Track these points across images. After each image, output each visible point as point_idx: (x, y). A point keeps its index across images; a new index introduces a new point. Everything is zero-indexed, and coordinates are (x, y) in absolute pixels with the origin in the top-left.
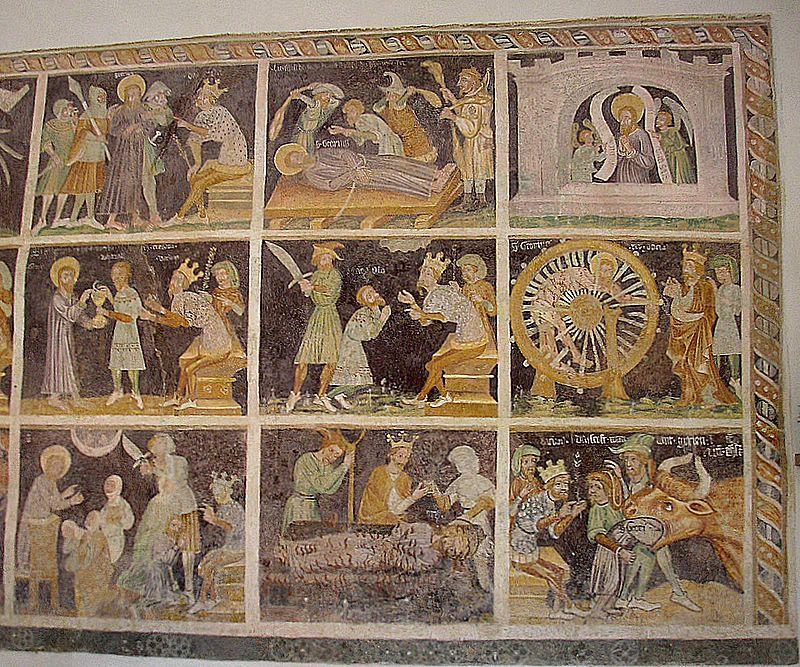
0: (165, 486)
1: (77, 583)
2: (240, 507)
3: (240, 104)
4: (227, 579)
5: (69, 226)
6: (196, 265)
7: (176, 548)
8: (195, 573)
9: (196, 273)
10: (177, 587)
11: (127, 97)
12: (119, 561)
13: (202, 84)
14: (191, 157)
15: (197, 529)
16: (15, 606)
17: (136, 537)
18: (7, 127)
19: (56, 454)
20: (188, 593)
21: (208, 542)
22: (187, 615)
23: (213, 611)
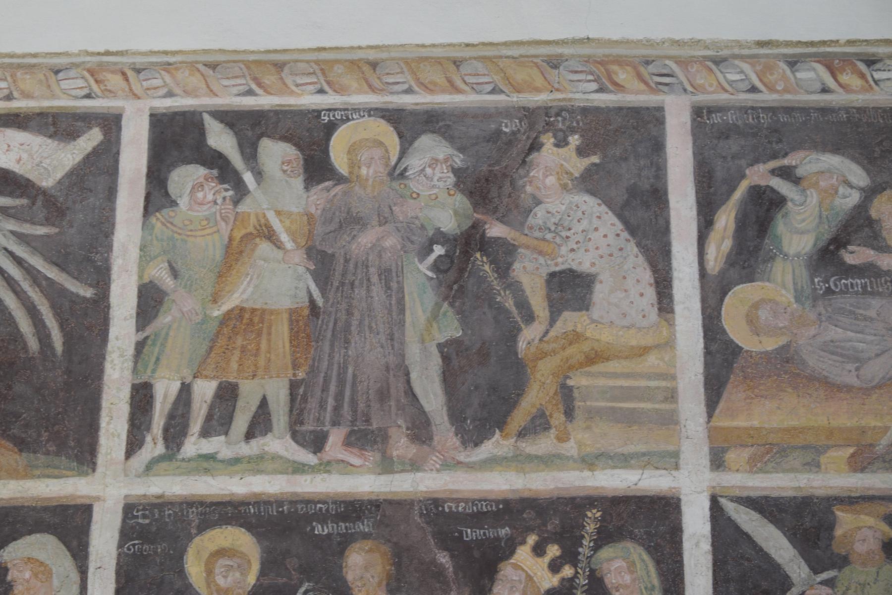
3: (633, 192)
5: (226, 453)
6: (554, 551)
9: (554, 567)
11: (353, 165)
13: (535, 146)
14: (524, 306)
18: (48, 222)
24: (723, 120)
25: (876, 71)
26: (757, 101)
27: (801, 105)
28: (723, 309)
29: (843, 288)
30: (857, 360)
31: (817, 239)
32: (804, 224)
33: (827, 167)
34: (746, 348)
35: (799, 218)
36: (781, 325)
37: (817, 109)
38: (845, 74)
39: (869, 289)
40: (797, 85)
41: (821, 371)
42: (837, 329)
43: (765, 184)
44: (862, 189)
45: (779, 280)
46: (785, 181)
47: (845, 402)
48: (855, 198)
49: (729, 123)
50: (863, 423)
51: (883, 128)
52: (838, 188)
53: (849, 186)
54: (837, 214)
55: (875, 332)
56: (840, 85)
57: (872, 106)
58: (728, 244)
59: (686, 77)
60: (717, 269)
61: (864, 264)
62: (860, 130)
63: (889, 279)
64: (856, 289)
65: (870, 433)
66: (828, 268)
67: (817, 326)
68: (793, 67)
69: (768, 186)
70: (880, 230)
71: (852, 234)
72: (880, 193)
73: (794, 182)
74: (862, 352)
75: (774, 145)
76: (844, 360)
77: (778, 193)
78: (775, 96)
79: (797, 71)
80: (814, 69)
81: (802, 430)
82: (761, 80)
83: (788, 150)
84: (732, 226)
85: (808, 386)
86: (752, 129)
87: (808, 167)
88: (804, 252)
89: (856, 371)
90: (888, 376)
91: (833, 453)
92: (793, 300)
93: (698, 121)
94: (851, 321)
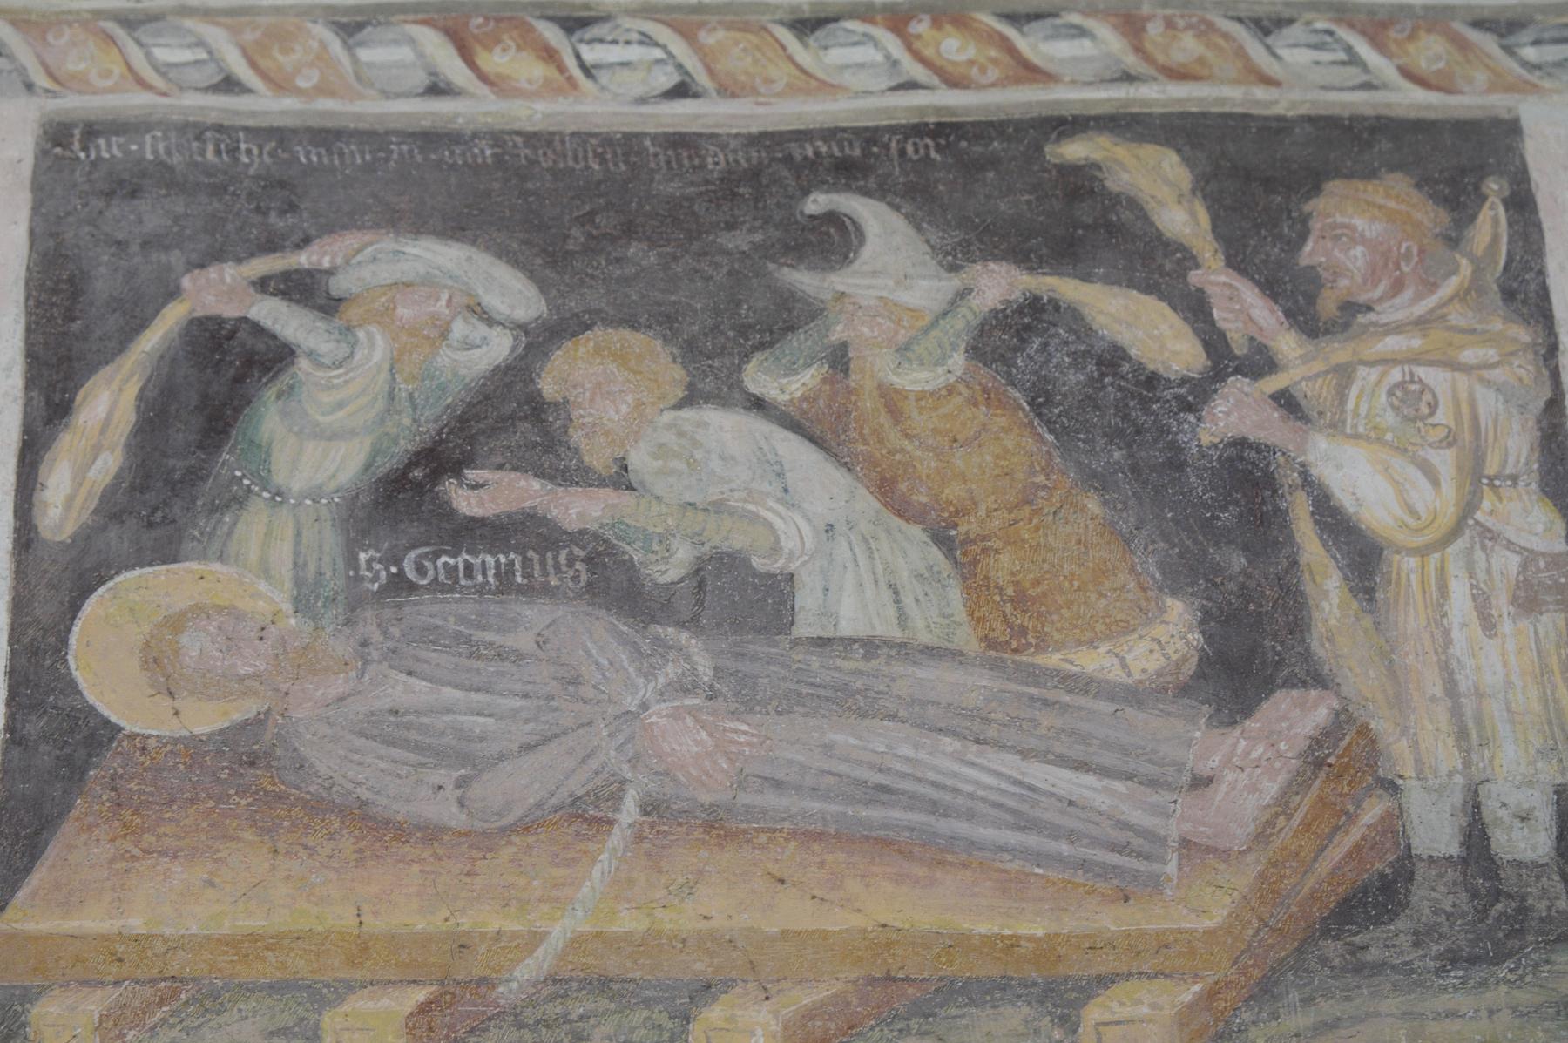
24: (127, 152)
25: (590, 42)
26: (236, 113)
27: (362, 126)
28: (76, 629)
29: (442, 577)
30: (466, 759)
31: (375, 453)
32: (341, 414)
33: (422, 271)
34: (129, 727)
35: (327, 398)
36: (242, 671)
37: (412, 135)
38: (498, 49)
39: (519, 579)
40: (359, 78)
41: (351, 786)
42: (412, 680)
43: (237, 314)
44: (522, 328)
45: (253, 556)
46: (294, 307)
47: (416, 868)
48: (499, 347)
49: (144, 159)
50: (466, 923)
51: (599, 183)
52: (449, 323)
53: (481, 319)
54: (443, 389)
55: (529, 688)
56: (483, 78)
57: (572, 128)
58: (108, 465)
59: (38, 56)
60: (70, 528)
61: (509, 516)
62: (530, 186)
63: (577, 551)
64: (480, 578)
65: (483, 949)
66: (402, 526)
67: (353, 674)
68: (351, 35)
69: (245, 320)
70: (566, 427)
71: (482, 439)
72: (575, 334)
73: (321, 309)
74: (482, 739)
75: (273, 218)
76: (424, 760)
77: (274, 337)
78: (289, 103)
79: (361, 44)
80: (411, 41)
81: (275, 942)
82: (253, 64)
83: (313, 232)
84: (127, 418)
85: (307, 826)
86: (209, 175)
87: (366, 273)
88: (333, 485)
89: (458, 786)
90: (554, 801)
91: (361, 1004)
92: (287, 607)
93: (56, 156)
94: (456, 659)
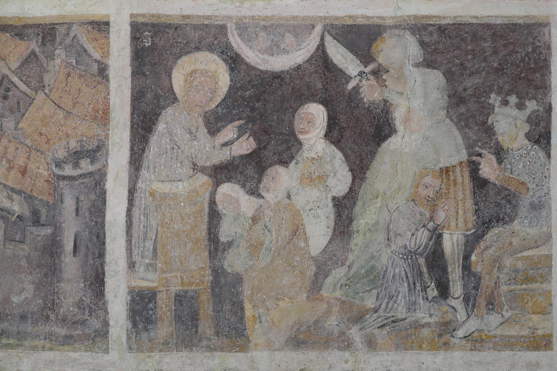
0: (407, 120)
1: (247, 292)
2: (542, 154)
4: (520, 277)
7: (431, 225)
8: (466, 267)
10: (436, 293)
12: (324, 251)
15: (468, 192)
16: (129, 338)
17: (357, 209)
19: (202, 67)
20: (453, 303)
21: (487, 213)
22: (454, 340)
23: (499, 332)
